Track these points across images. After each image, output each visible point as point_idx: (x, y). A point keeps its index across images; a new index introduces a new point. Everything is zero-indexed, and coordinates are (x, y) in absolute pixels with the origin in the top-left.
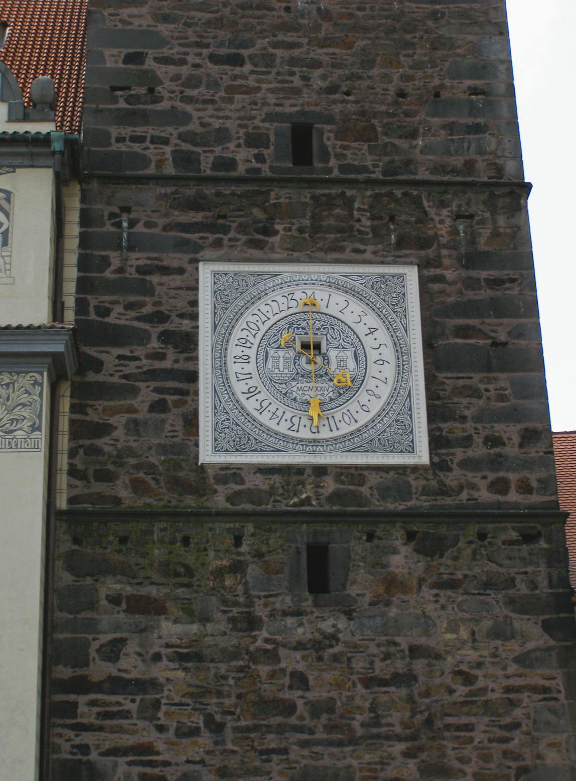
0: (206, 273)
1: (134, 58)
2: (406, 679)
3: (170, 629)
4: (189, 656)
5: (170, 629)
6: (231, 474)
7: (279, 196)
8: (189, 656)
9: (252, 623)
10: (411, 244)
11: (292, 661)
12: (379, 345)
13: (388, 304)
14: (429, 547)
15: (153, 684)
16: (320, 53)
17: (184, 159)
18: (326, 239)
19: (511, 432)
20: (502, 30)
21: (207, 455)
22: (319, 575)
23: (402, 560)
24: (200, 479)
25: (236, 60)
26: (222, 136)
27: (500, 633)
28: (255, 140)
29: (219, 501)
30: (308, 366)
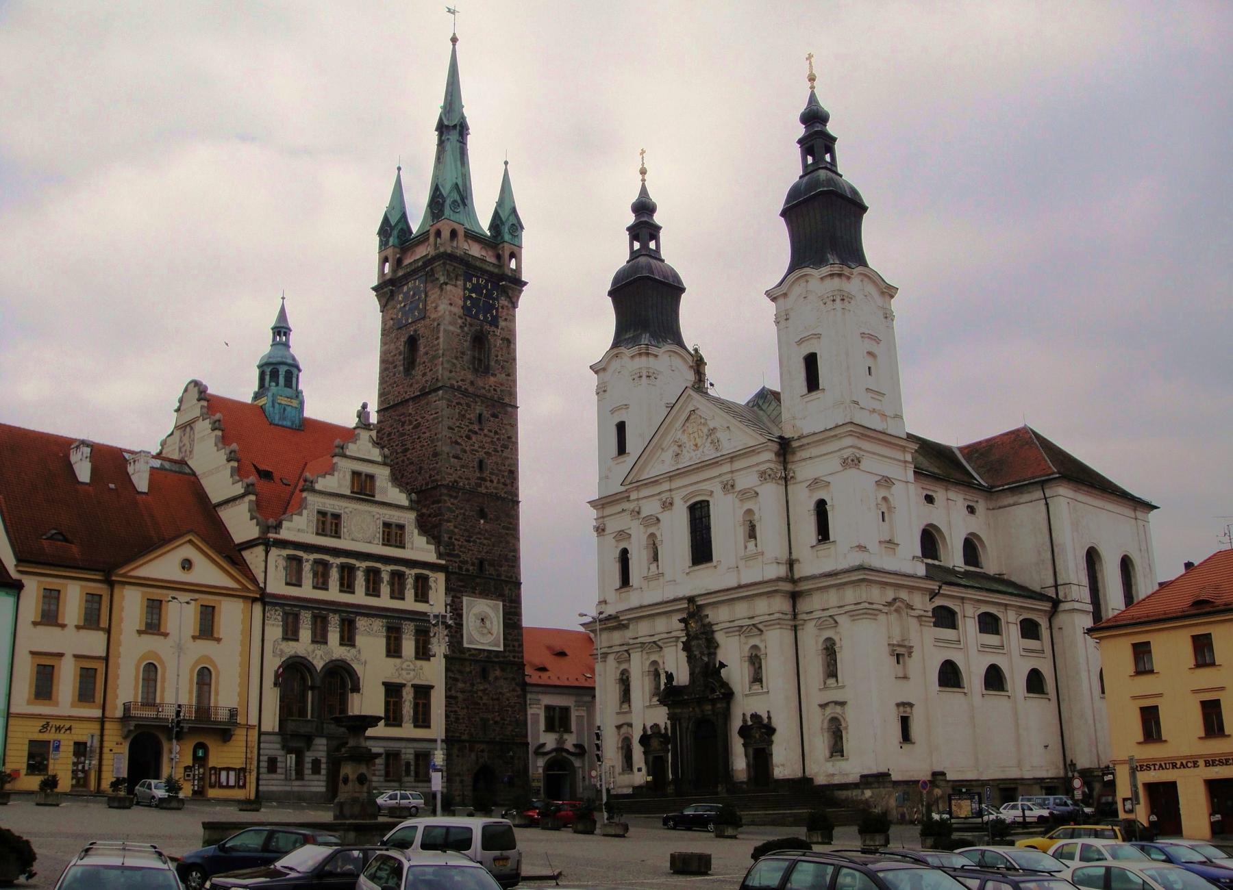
0: (465, 599)
1: (450, 538)
2: (498, 699)
3: (460, 685)
4: (463, 691)
5: (460, 685)
6: (469, 649)
7: (478, 580)
8: (463, 691)
9: (473, 685)
10: (500, 596)
11: (480, 694)
12: (495, 620)
13: (495, 608)
14: (503, 670)
15: (456, 698)
16: (485, 542)
17: (460, 568)
18: (485, 593)
19: (516, 644)
20: (518, 540)
21: (466, 645)
22: (484, 674)
23: (498, 673)
24: (463, 650)
25: (469, 541)
26: (465, 562)
27: (514, 690)
28: (473, 564)
29: (467, 655)
30: (482, 624)
